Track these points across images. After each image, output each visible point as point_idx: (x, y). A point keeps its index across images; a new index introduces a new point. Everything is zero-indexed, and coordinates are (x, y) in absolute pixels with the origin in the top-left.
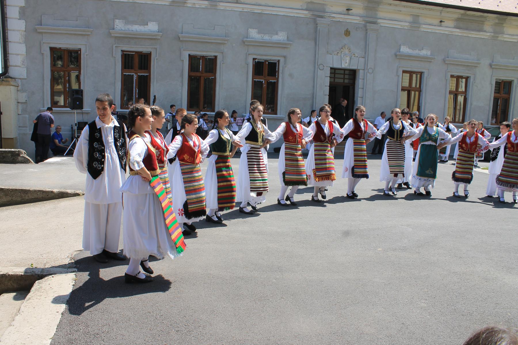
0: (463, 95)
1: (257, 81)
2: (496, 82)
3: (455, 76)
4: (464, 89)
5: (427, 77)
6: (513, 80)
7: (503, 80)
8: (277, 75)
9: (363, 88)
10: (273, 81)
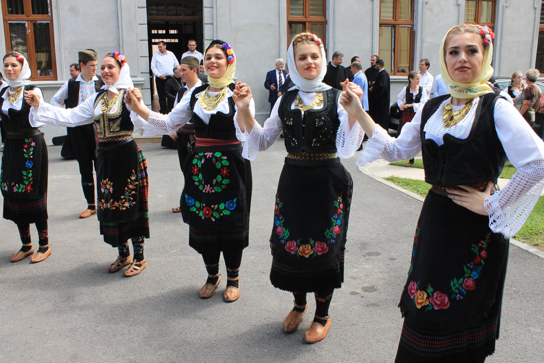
1: (15, 23)
8: (49, 10)
9: (212, 24)
10: (43, 22)
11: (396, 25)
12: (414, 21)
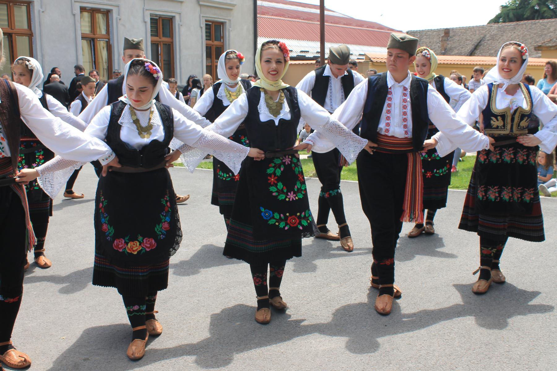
0: (105, 40)
2: (151, 19)
3: (87, 9)
4: (104, 32)
5: (39, 11)
6: (174, 17)
7: (161, 16)
11: (94, 38)
12: (110, 35)
